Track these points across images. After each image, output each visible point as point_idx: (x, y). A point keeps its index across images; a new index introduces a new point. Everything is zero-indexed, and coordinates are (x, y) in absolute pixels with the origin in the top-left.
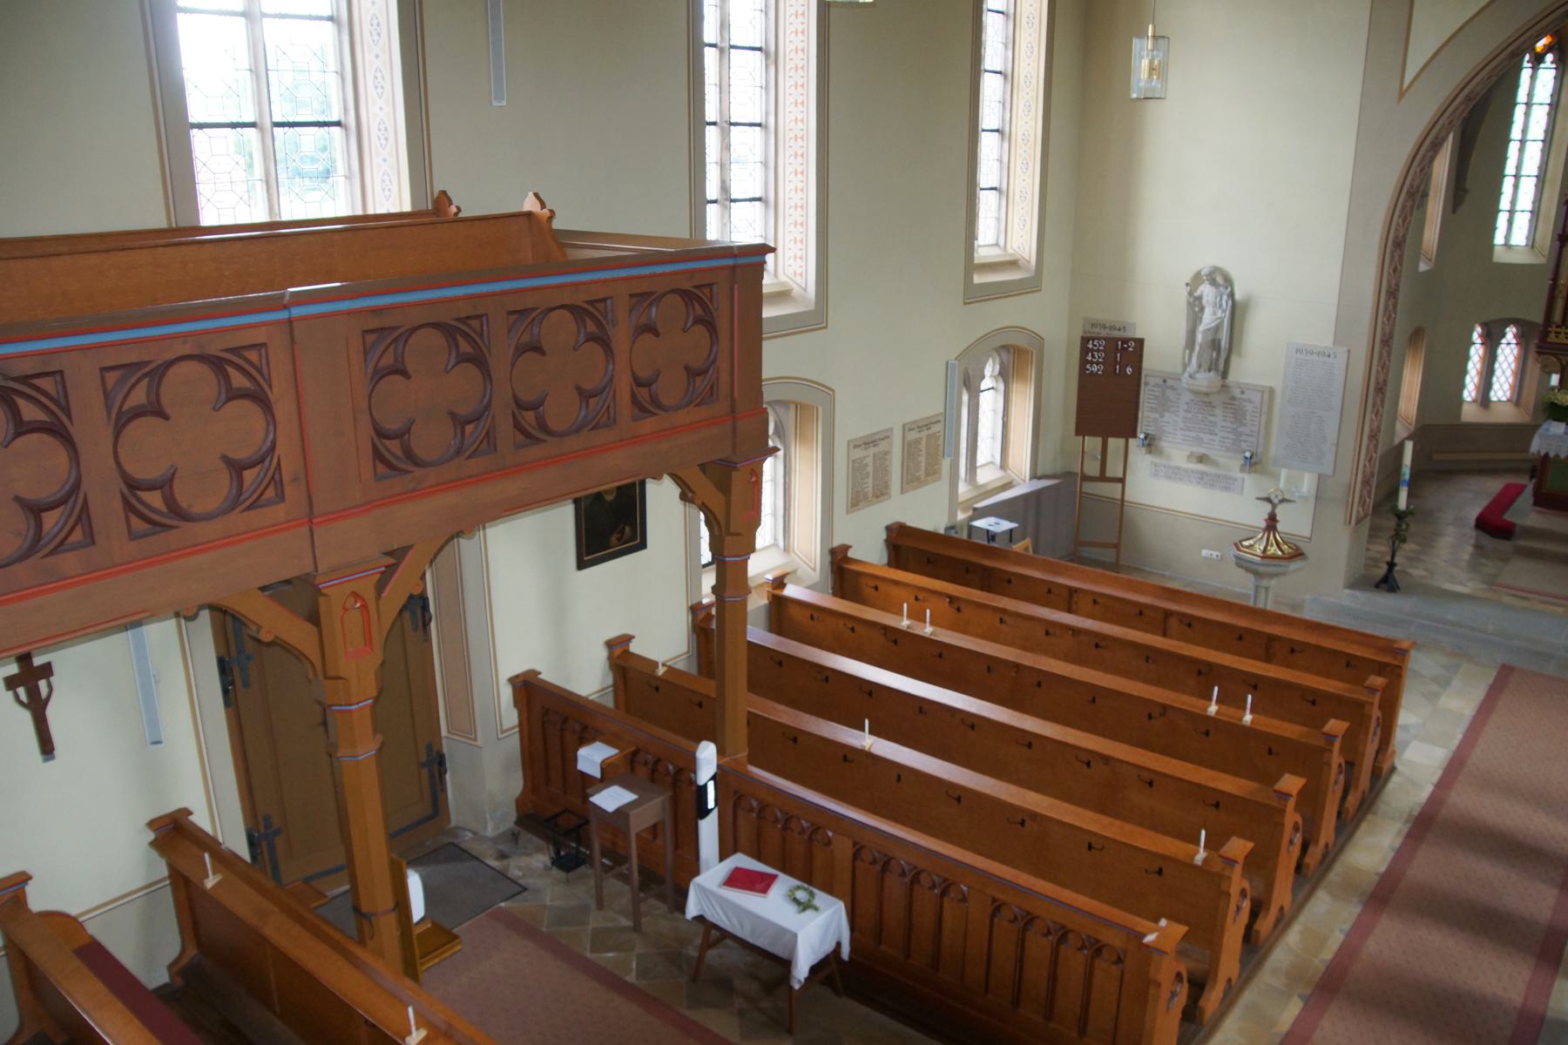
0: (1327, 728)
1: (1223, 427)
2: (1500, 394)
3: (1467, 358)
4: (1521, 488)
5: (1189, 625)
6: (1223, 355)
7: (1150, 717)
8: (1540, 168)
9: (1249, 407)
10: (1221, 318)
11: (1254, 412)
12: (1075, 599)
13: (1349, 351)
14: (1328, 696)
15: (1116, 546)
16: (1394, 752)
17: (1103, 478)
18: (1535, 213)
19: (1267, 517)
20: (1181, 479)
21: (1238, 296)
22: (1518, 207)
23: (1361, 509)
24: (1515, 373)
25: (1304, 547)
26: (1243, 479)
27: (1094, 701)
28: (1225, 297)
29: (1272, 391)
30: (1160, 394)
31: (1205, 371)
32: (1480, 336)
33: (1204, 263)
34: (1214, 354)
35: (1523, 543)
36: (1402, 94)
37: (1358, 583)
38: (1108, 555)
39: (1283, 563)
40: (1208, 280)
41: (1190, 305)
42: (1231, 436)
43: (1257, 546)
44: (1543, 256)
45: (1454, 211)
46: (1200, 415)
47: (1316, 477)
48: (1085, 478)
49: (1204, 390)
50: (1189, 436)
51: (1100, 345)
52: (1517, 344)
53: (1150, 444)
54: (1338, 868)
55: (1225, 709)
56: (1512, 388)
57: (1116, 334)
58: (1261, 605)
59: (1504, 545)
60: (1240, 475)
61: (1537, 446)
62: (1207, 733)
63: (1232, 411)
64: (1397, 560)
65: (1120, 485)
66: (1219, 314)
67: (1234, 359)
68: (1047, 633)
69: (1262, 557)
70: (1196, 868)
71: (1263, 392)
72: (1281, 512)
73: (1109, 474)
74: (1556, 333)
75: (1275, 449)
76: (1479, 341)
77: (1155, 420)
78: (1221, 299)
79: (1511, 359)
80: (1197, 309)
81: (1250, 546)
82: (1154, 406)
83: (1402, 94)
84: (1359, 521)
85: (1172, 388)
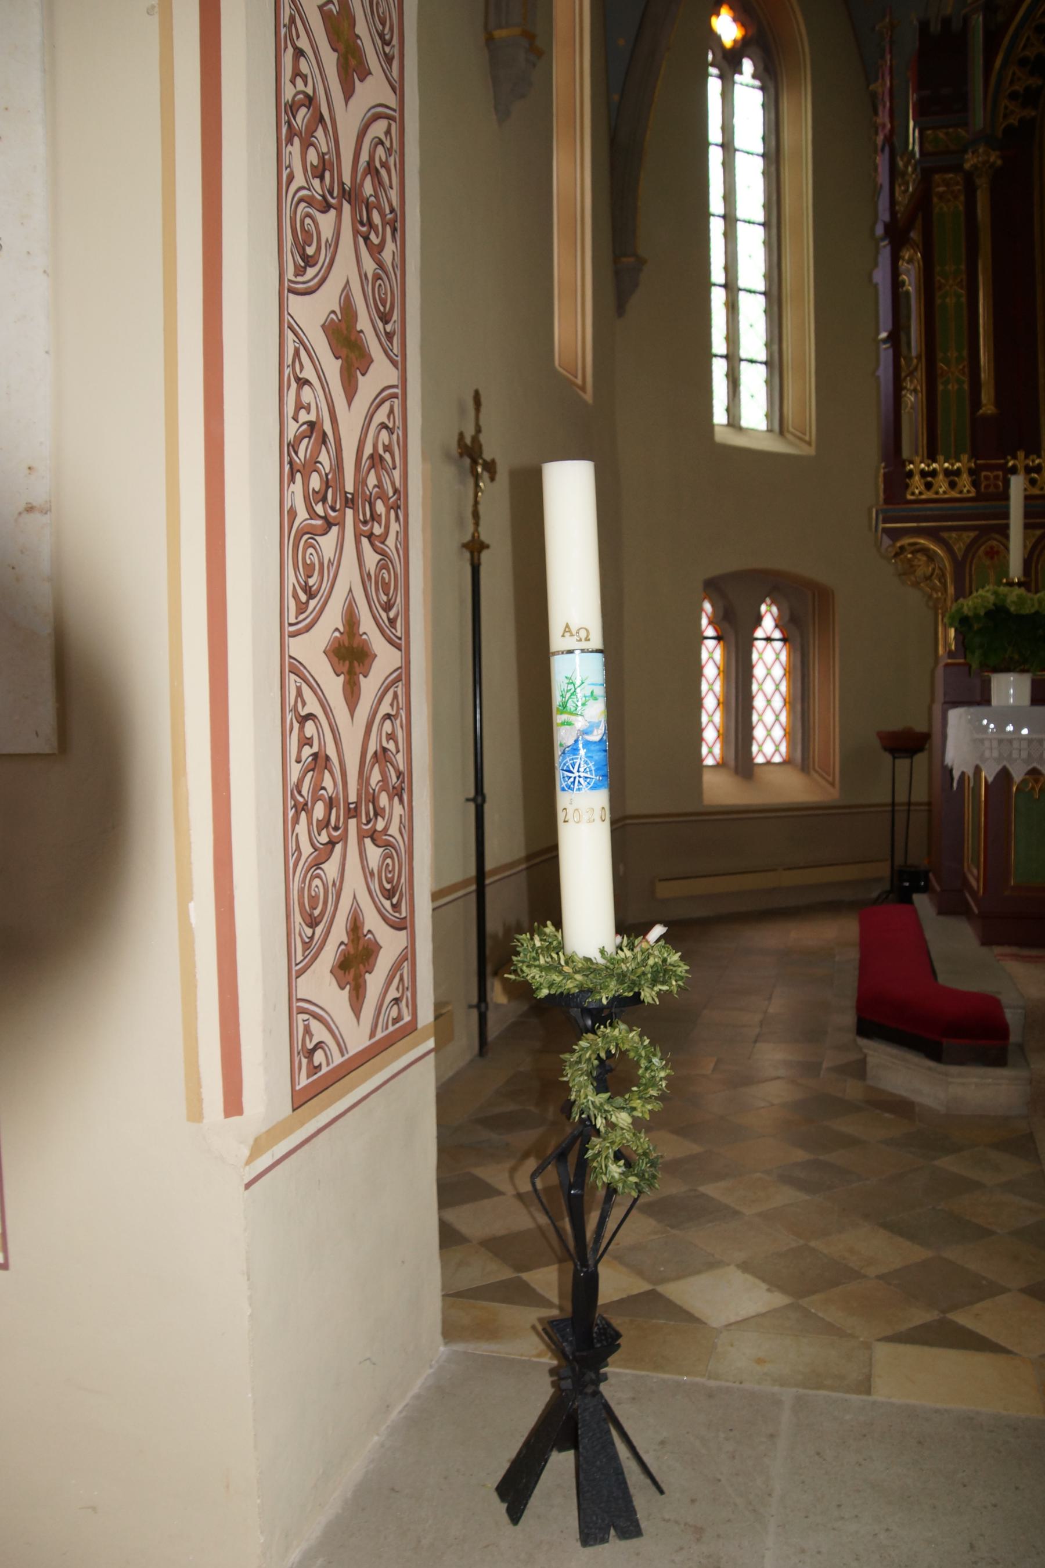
2: (769, 748)
18: (775, 365)
32: (710, 622)
44: (809, 443)
45: (621, 308)
52: (784, 640)
56: (789, 734)
76: (710, 632)
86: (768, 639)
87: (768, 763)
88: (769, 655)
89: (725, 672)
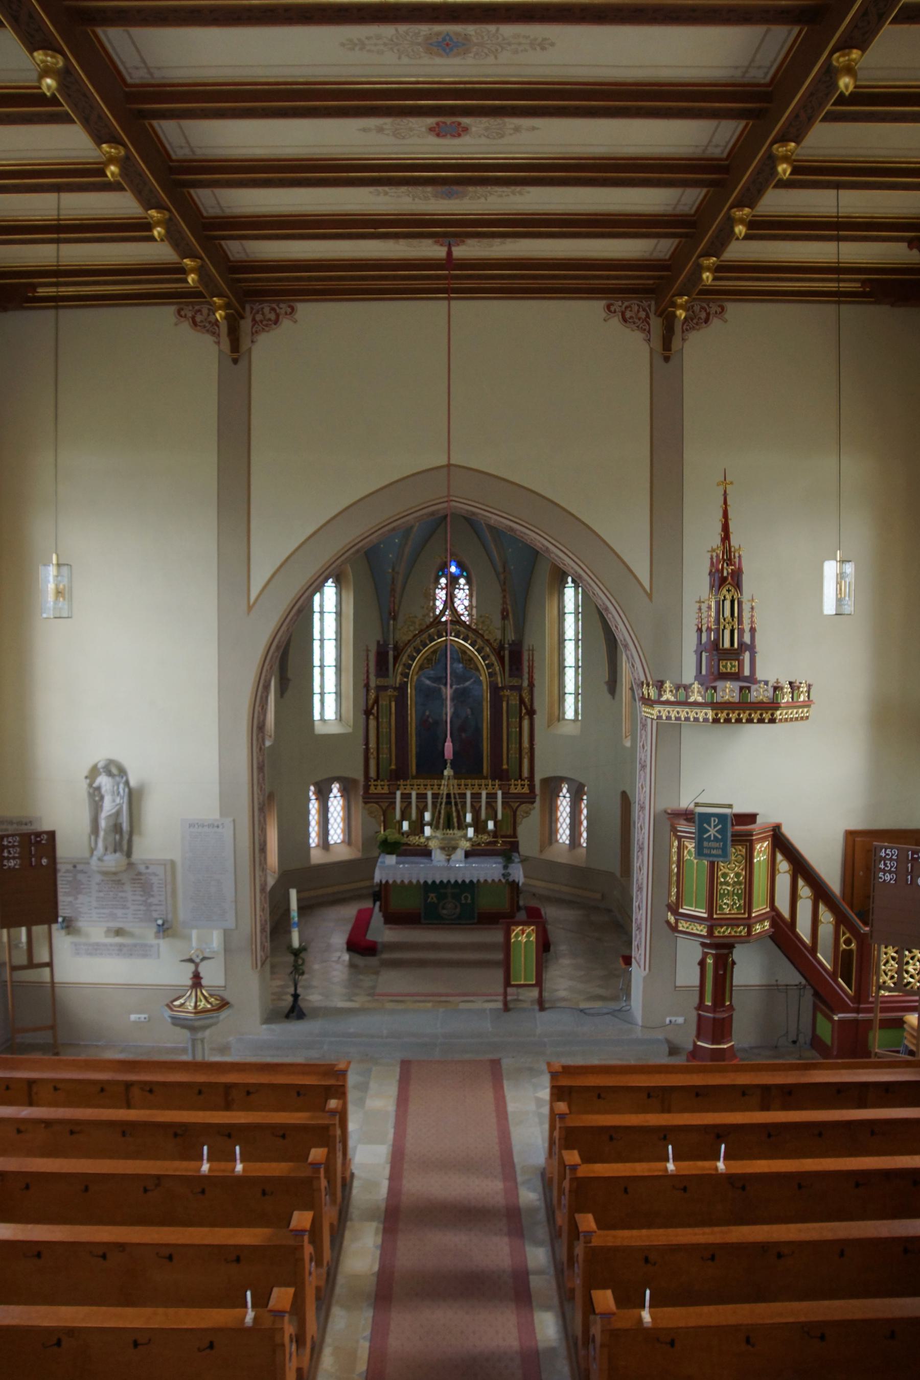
0: (311, 1159)
1: (133, 901)
2: (335, 837)
3: (308, 812)
4: (371, 911)
5: (151, 1091)
6: (126, 837)
7: (146, 1190)
8: (336, 660)
9: (154, 880)
10: (119, 804)
11: (159, 883)
12: (35, 1089)
13: (234, 821)
14: (304, 1128)
15: (53, 1027)
16: (350, 1160)
17: (32, 965)
18: (339, 694)
19: (191, 975)
20: (101, 954)
21: (132, 783)
22: (326, 691)
23: (262, 953)
24: (343, 820)
25: (227, 996)
26: (158, 945)
27: (86, 1189)
28: (121, 786)
29: (173, 863)
30: (70, 879)
31: (111, 853)
32: (314, 793)
33: (100, 756)
34: (117, 837)
35: (386, 956)
36: (250, 608)
37: (272, 1016)
38: (44, 1037)
39: (215, 1014)
40: (104, 772)
41: (91, 796)
42: (142, 908)
43: (188, 1003)
46: (111, 893)
47: (222, 931)
48: (14, 968)
49: (113, 869)
50: (104, 914)
51: (15, 841)
52: (341, 796)
53: (69, 926)
54: (341, 1280)
55: (216, 1165)
56: (343, 831)
57: (25, 829)
58: (199, 1058)
59: (373, 961)
60: (155, 942)
61: (379, 876)
62: (203, 1192)
63: (139, 885)
64: (299, 991)
65: (47, 970)
66: (118, 800)
67: (135, 839)
68: (19, 1131)
69: (195, 1013)
70: (249, 1329)
71: (165, 865)
72: (205, 970)
73: (36, 960)
74: (374, 785)
75: (183, 914)
76: (313, 797)
77: (71, 902)
78: (118, 788)
79: (339, 808)
80: (97, 798)
81: (182, 1005)
82: (67, 890)
83: (250, 608)
84: (263, 964)
85: (82, 872)
86: (335, 797)
87: (336, 843)
88: (335, 803)
89: (319, 811)
